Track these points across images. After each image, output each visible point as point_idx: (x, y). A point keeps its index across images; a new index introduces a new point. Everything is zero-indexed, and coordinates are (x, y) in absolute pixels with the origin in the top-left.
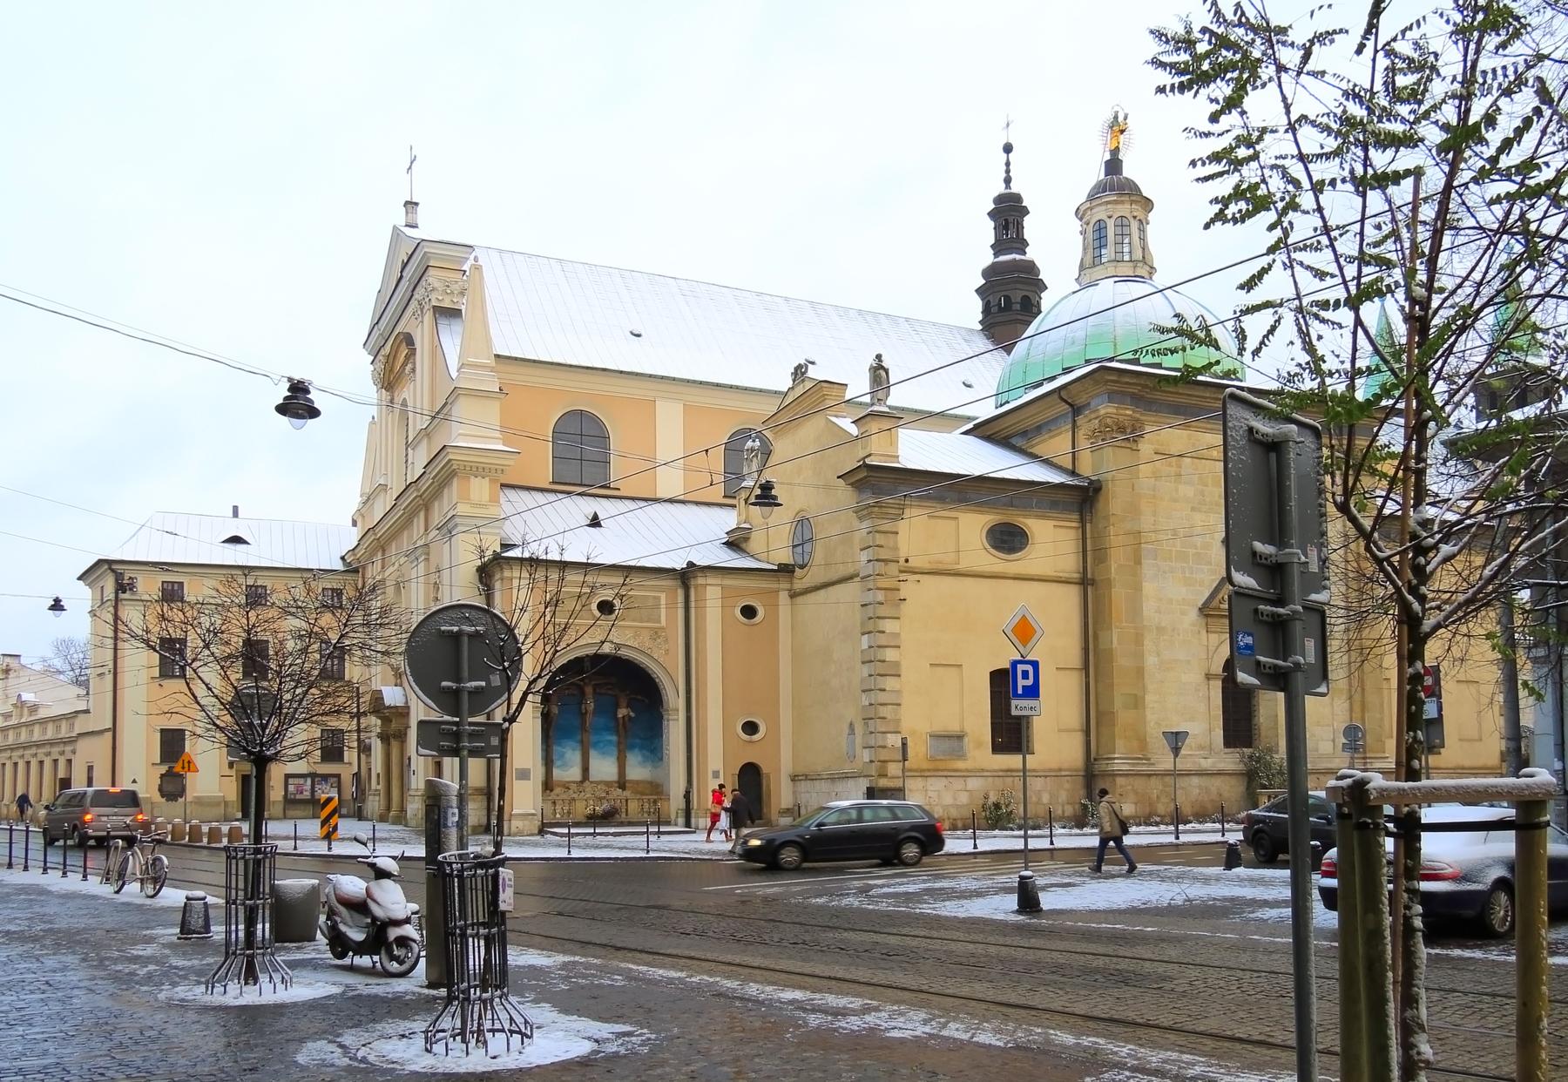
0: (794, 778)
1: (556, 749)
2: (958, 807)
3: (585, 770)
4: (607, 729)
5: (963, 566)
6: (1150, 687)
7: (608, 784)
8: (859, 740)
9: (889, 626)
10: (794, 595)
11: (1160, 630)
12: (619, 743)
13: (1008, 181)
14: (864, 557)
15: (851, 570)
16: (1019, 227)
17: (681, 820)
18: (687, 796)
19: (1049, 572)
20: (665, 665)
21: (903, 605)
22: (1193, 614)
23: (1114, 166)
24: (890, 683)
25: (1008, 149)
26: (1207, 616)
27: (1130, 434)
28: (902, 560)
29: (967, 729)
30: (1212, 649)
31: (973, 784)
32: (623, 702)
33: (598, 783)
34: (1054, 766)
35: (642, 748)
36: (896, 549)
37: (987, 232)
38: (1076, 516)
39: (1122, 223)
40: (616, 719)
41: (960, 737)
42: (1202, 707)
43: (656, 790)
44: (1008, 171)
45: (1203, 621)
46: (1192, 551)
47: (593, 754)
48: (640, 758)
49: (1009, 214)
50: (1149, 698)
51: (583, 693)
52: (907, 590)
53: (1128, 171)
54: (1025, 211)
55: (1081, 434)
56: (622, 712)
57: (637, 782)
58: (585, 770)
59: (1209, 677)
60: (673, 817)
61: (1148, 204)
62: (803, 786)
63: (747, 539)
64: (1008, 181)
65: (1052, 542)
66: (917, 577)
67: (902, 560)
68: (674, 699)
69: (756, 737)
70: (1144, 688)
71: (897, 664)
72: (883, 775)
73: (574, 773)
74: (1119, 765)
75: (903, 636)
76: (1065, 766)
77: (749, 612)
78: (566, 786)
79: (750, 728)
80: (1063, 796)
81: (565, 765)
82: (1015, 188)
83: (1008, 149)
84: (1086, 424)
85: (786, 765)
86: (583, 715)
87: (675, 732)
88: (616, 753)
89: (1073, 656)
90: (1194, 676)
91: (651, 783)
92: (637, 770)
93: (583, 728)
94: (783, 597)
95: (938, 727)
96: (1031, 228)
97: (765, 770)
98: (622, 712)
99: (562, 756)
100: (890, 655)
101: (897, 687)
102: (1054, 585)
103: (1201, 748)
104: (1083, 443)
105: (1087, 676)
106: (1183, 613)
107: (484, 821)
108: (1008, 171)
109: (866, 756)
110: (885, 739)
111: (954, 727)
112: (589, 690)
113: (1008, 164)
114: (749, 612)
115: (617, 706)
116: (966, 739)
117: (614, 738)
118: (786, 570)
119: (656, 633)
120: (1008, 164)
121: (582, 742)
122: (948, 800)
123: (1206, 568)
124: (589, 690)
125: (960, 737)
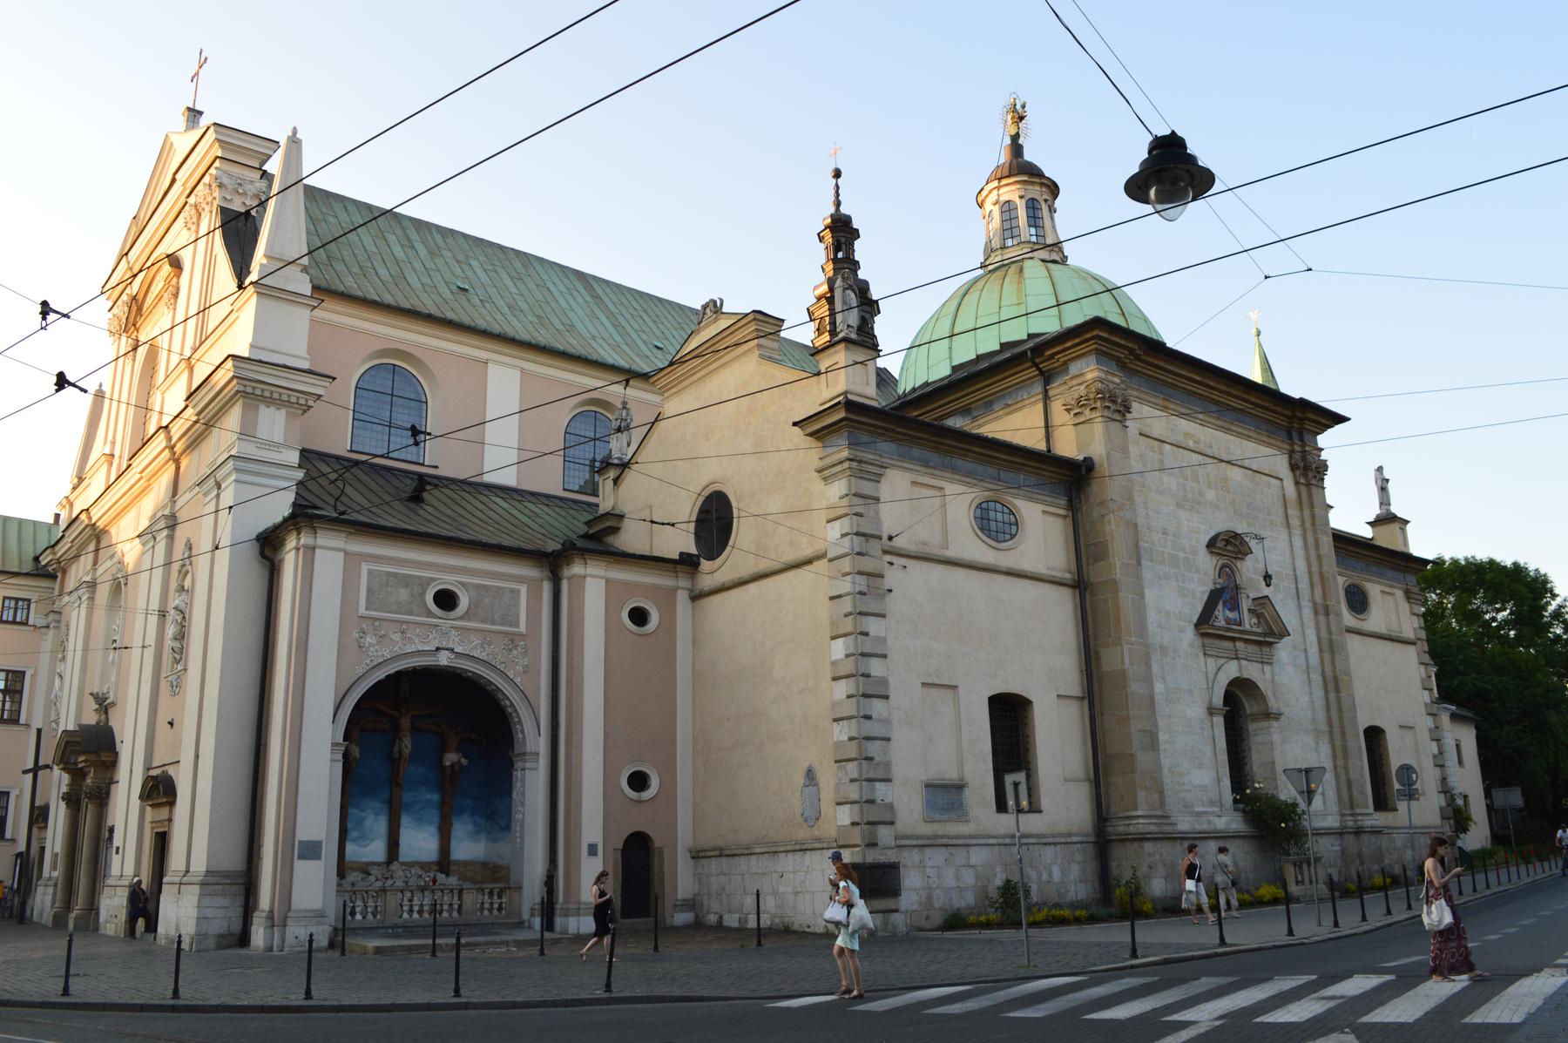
0: (697, 855)
1: (352, 811)
2: (961, 890)
5: (951, 553)
6: (1161, 723)
7: (424, 866)
8: (827, 793)
9: (874, 626)
10: (696, 597)
11: (1163, 649)
13: (838, 204)
14: (834, 531)
15: (807, 551)
16: (850, 249)
17: (537, 922)
19: (1040, 568)
21: (890, 598)
22: (1190, 632)
23: (1016, 148)
24: (877, 707)
25: (837, 174)
26: (1203, 635)
27: (1118, 408)
28: (885, 537)
29: (968, 777)
30: (1211, 676)
31: (978, 857)
33: (411, 864)
34: (1063, 828)
36: (877, 520)
37: (818, 255)
38: (1063, 502)
39: (1032, 205)
41: (959, 787)
42: (1208, 751)
43: (496, 877)
44: (837, 194)
45: (1199, 641)
46: (1182, 555)
47: (405, 820)
48: (470, 827)
49: (842, 232)
50: (1163, 737)
51: (396, 729)
52: (893, 578)
53: (1029, 156)
54: (855, 234)
55: (1057, 407)
56: (451, 758)
57: (466, 864)
59: (1211, 711)
60: (526, 915)
61: (1054, 189)
62: (714, 865)
63: (615, 530)
64: (838, 204)
65: (1041, 533)
66: (903, 561)
67: (885, 537)
68: (533, 738)
69: (647, 795)
70: (1155, 724)
71: (884, 682)
72: (872, 845)
73: (375, 850)
74: (1142, 826)
75: (890, 641)
76: (1075, 829)
77: (639, 617)
78: (365, 869)
79: (639, 781)
80: (1075, 871)
81: (364, 838)
82: (844, 210)
83: (837, 174)
84: (1063, 393)
85: (685, 836)
86: (394, 762)
87: (532, 785)
88: (437, 819)
89: (1072, 682)
90: (1197, 711)
91: (484, 864)
92: (468, 847)
93: (394, 782)
94: (682, 597)
95: (932, 774)
96: (861, 250)
97: (657, 843)
98: (451, 758)
99: (361, 821)
100: (876, 668)
101: (885, 715)
102: (1054, 587)
103: (1212, 803)
104: (1059, 414)
105: (1091, 707)
106: (1182, 631)
107: (237, 927)
108: (837, 194)
109: (845, 816)
110: (873, 790)
111: (951, 774)
112: (405, 723)
113: (837, 187)
114: (639, 617)
115: (444, 749)
116: (967, 792)
117: (435, 797)
118: (687, 563)
119: (513, 639)
120: (837, 187)
121: (390, 803)
122: (950, 881)
123: (1196, 576)
125: (959, 787)
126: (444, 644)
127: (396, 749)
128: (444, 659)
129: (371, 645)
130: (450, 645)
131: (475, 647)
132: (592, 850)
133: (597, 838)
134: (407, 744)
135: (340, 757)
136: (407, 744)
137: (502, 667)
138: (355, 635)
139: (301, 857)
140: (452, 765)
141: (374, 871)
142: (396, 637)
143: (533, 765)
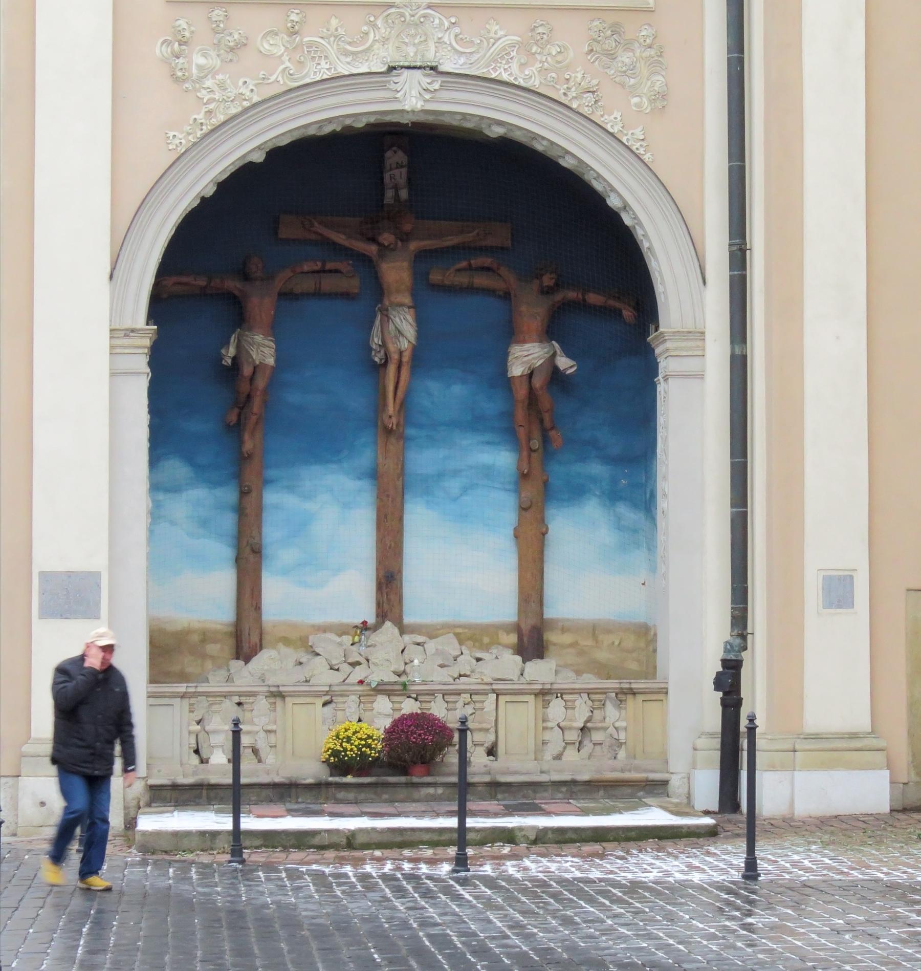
3: (389, 582)
4: (475, 423)
7: (475, 637)
12: (524, 476)
18: (729, 680)
20: (654, 172)
32: (532, 311)
33: (432, 632)
35: (613, 496)
40: (507, 383)
47: (418, 518)
48: (605, 535)
51: (377, 291)
56: (526, 356)
57: (595, 630)
58: (389, 582)
88: (509, 517)
98: (526, 356)
99: (300, 528)
112: (396, 272)
115: (510, 333)
117: (503, 459)
121: (375, 475)
124: (396, 272)
126: (411, 55)
127: (376, 340)
128: (411, 99)
129: (206, 72)
130: (430, 56)
131: (504, 55)
132: (838, 592)
133: (854, 558)
134: (402, 328)
135: (141, 363)
136: (402, 328)
137: (583, 104)
138: (159, 50)
139: (48, 612)
140: (531, 375)
141: (332, 647)
142: (276, 46)
143: (690, 365)
